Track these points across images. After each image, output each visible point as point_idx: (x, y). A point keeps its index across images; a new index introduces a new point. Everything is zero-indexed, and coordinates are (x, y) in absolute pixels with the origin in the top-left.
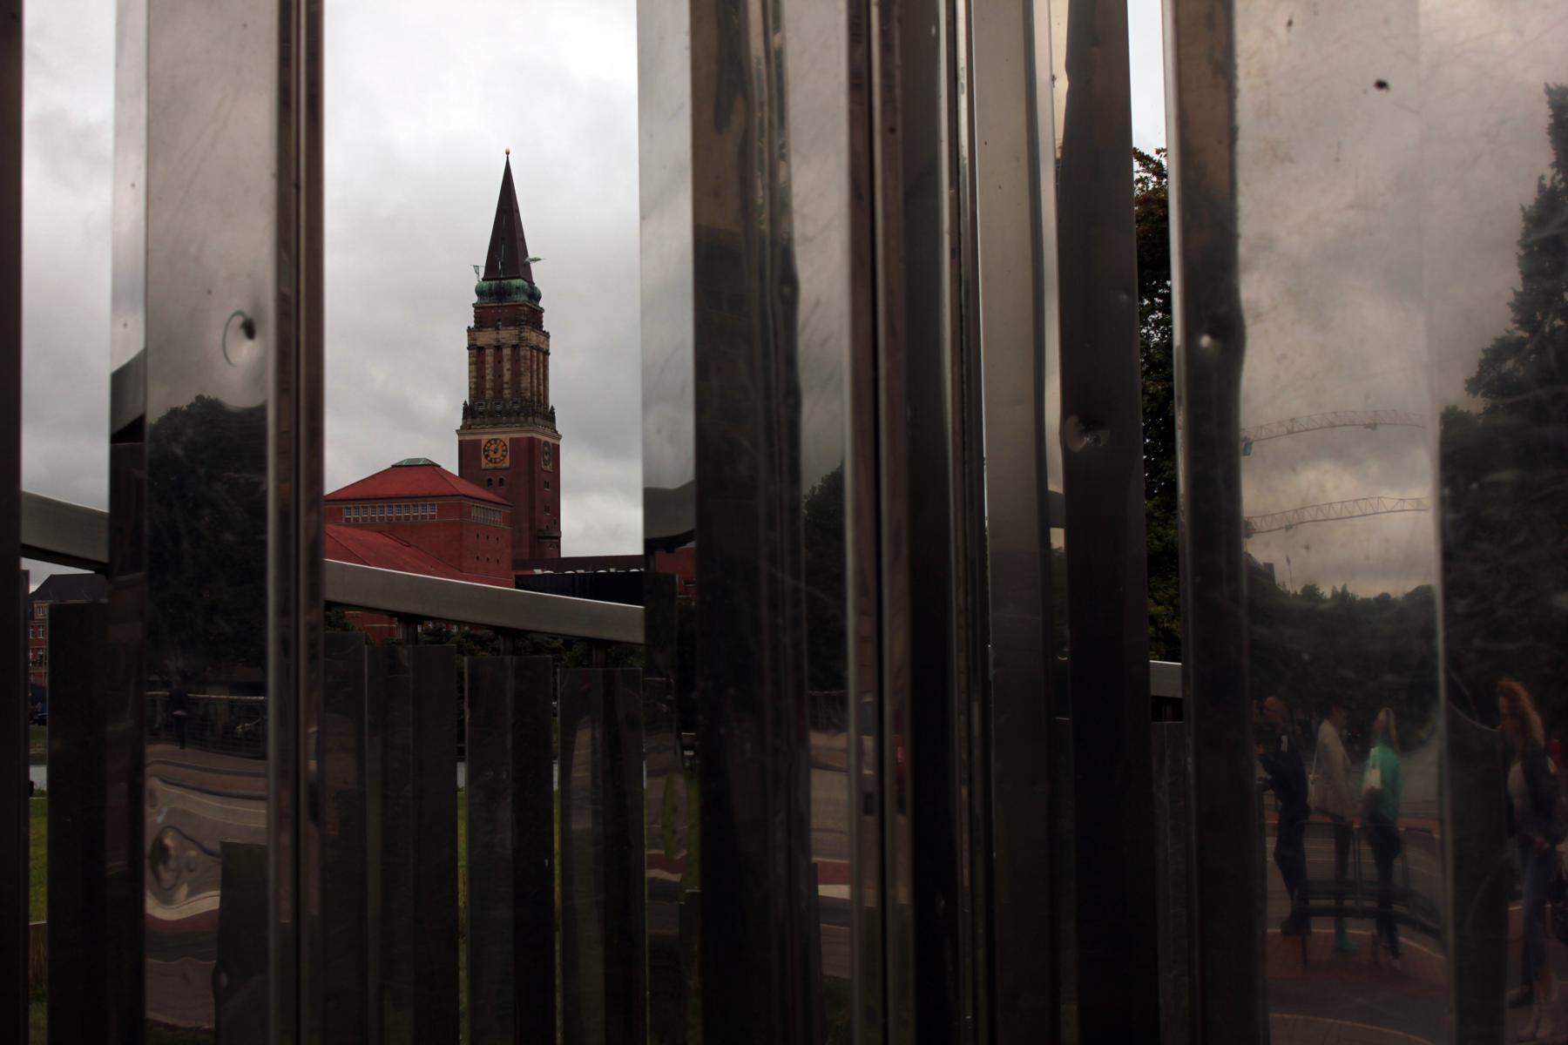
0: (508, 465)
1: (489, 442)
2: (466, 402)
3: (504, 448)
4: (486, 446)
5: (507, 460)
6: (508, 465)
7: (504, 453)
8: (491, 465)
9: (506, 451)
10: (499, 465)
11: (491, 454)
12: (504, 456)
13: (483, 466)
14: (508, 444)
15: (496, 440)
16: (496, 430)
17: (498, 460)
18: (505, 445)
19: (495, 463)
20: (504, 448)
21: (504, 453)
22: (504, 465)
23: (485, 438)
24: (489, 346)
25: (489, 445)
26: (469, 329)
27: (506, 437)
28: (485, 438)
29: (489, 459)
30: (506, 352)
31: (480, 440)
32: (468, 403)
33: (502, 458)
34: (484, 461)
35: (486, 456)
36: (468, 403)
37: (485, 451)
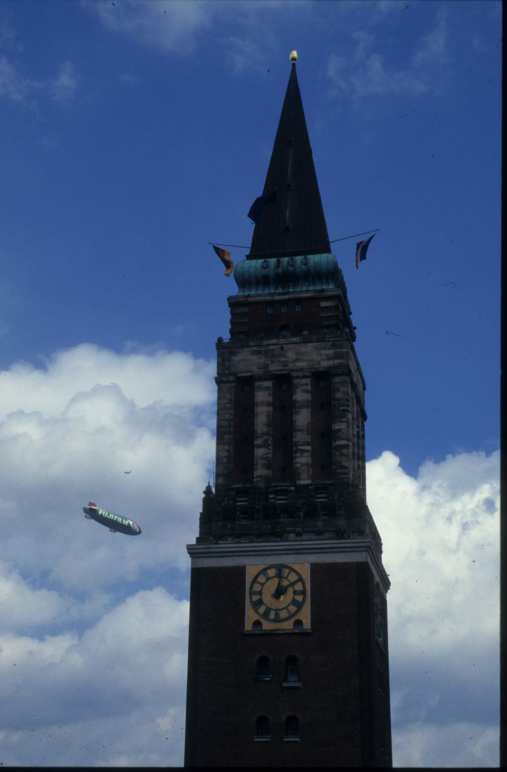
1: (264, 571)
2: (209, 488)
3: (299, 587)
4: (255, 580)
6: (307, 625)
7: (299, 598)
8: (267, 626)
9: (303, 593)
10: (288, 625)
11: (267, 598)
12: (299, 606)
13: (248, 627)
14: (307, 576)
16: (282, 545)
17: (284, 614)
18: (301, 579)
19: (277, 620)
21: (299, 598)
25: (262, 579)
27: (303, 566)
29: (262, 610)
32: (213, 490)
33: (293, 609)
34: (250, 616)
36: (213, 490)
37: (252, 593)
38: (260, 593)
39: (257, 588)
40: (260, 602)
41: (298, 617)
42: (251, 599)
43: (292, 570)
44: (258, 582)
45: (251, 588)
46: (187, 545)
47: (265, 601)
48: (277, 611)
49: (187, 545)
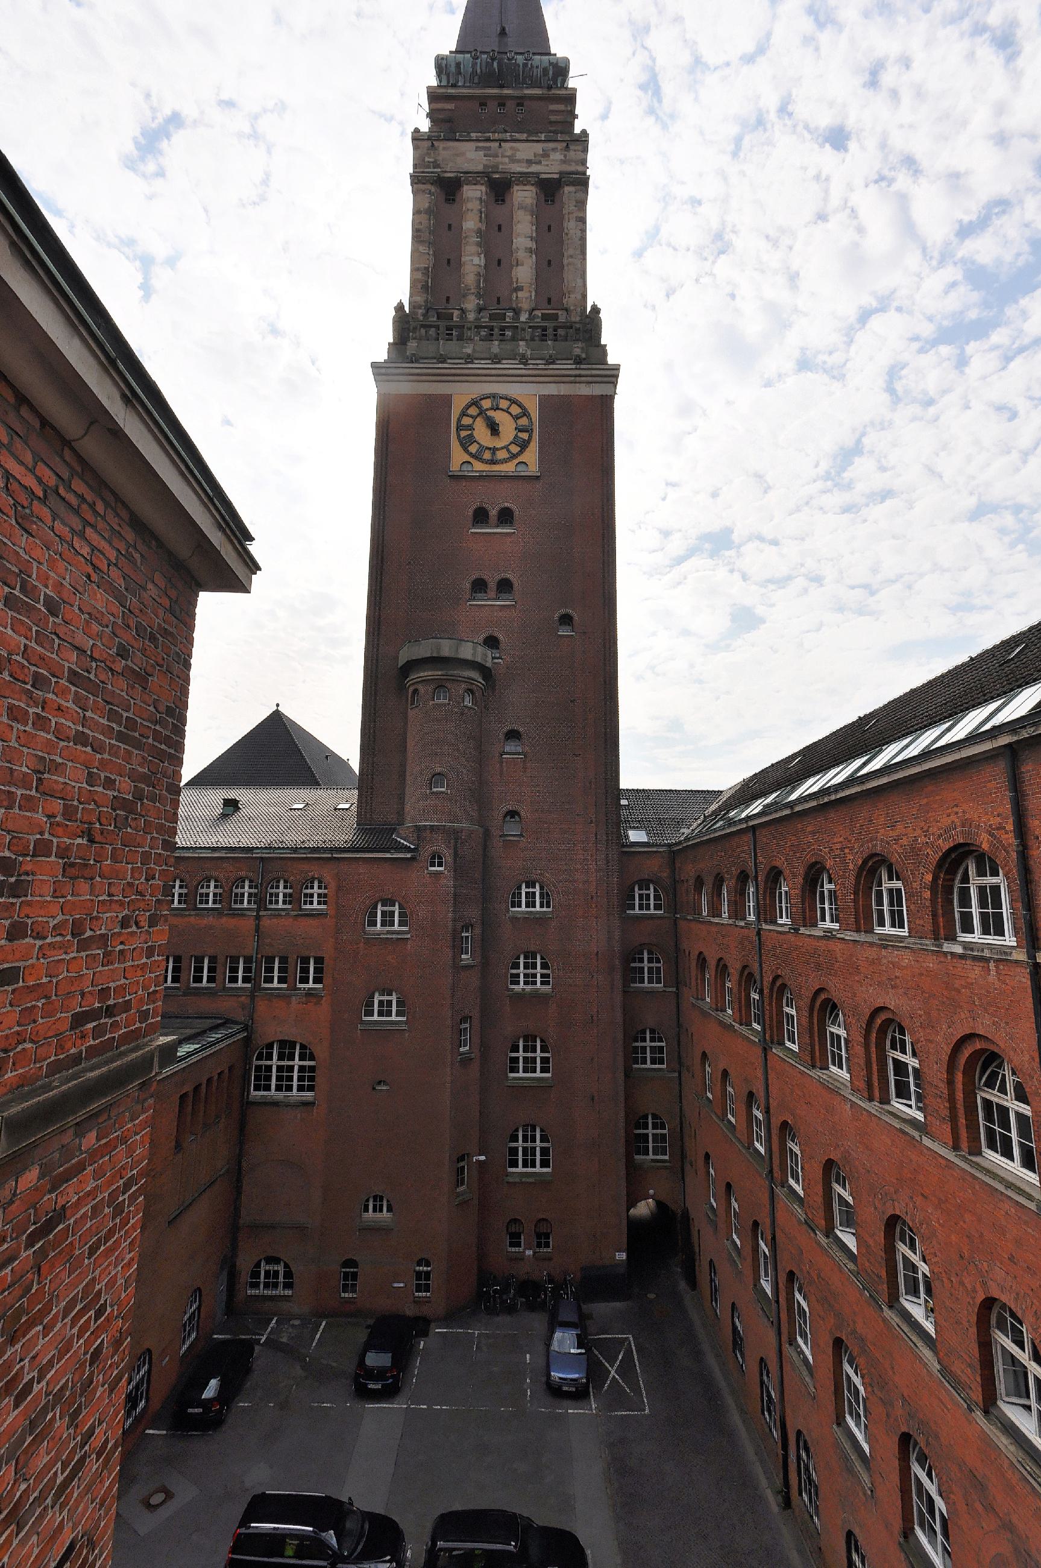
0: (533, 469)
1: (475, 403)
3: (524, 421)
4: (464, 414)
5: (531, 456)
6: (533, 469)
9: (528, 430)
10: (509, 468)
11: (481, 432)
12: (524, 445)
13: (455, 466)
15: (493, 396)
17: (502, 455)
18: (525, 413)
19: (493, 462)
20: (524, 421)
21: (525, 436)
22: (523, 471)
23: (462, 394)
24: (473, 177)
26: (417, 137)
28: (462, 394)
29: (473, 449)
30: (524, 196)
31: (446, 401)
33: (515, 449)
34: (458, 457)
35: (466, 443)
37: (460, 427)
38: (470, 427)
39: (466, 421)
40: (471, 439)
41: (520, 459)
42: (459, 436)
43: (514, 402)
44: (468, 416)
45: (459, 420)
46: (372, 363)
47: (475, 434)
48: (494, 450)
49: (372, 363)
